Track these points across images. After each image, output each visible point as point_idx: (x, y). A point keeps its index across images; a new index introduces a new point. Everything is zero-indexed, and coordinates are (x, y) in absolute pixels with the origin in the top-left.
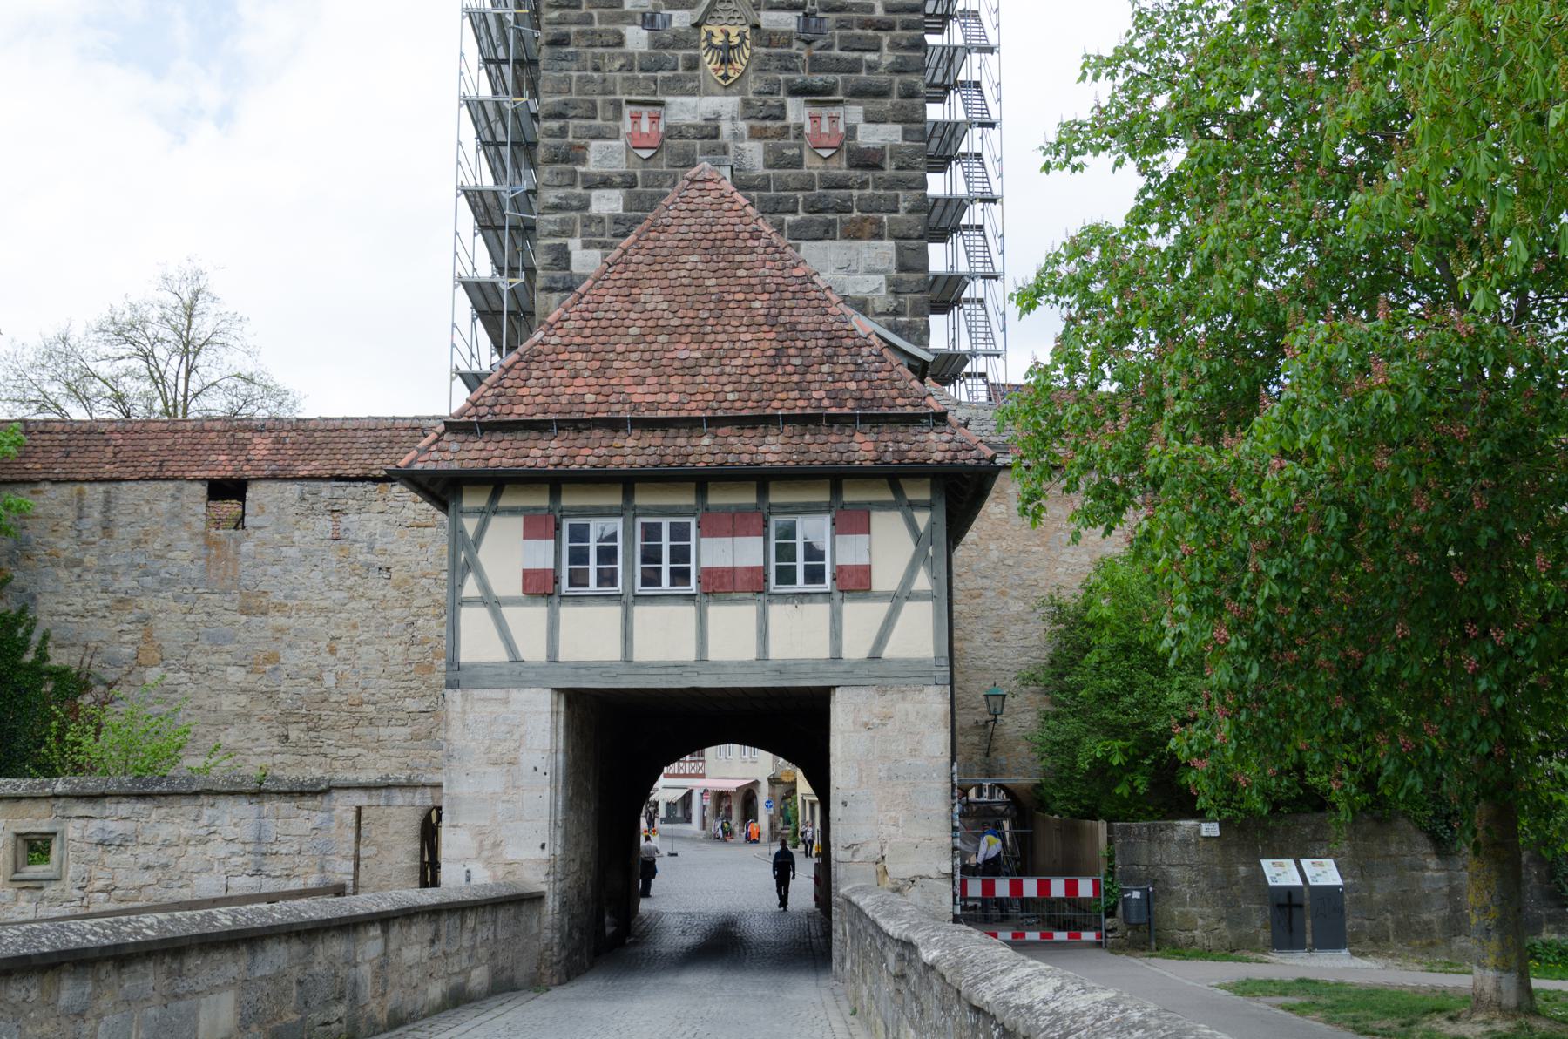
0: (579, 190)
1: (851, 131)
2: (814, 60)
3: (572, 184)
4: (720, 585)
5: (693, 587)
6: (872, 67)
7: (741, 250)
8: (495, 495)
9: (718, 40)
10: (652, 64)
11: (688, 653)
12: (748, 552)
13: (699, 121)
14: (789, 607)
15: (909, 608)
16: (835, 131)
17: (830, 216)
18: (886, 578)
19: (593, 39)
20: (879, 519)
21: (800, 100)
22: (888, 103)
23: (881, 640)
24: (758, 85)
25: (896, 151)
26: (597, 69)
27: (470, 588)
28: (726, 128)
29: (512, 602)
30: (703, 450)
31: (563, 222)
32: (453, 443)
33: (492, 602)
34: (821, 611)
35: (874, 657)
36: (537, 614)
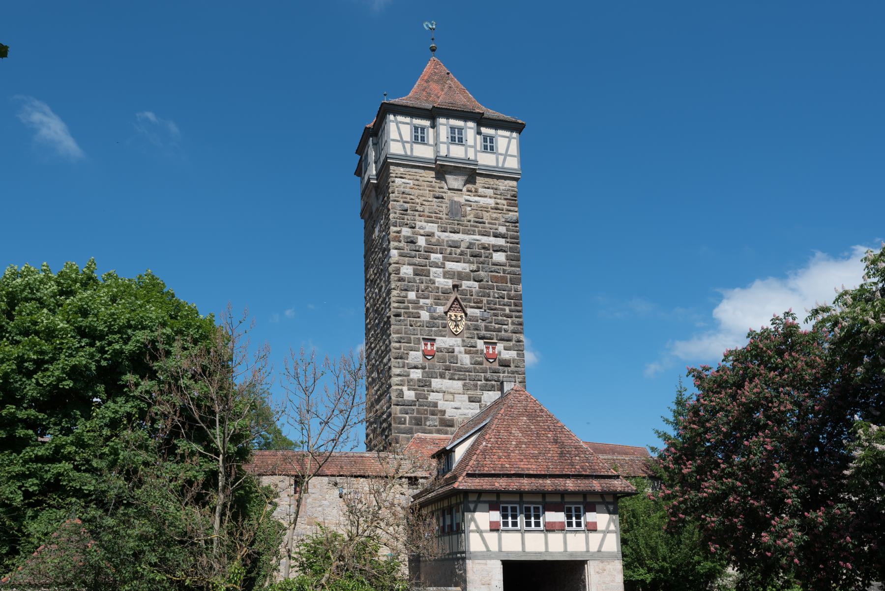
0: (406, 369)
1: (500, 353)
2: (486, 327)
3: (403, 367)
4: (551, 528)
5: (542, 527)
6: (506, 331)
7: (538, 416)
8: (479, 497)
9: (453, 318)
10: (430, 325)
11: (543, 549)
12: (558, 517)
13: (447, 346)
14: (573, 535)
15: (608, 535)
16: (494, 353)
17: (493, 383)
18: (601, 526)
19: (409, 315)
20: (598, 507)
21: (482, 341)
22: (511, 344)
23: (601, 545)
24: (468, 335)
25: (514, 360)
26: (411, 326)
27: (473, 527)
28: (457, 349)
29: (486, 531)
30: (548, 484)
31: (401, 381)
32: (470, 480)
33: (480, 531)
34: (581, 536)
35: (599, 551)
36: (495, 534)
